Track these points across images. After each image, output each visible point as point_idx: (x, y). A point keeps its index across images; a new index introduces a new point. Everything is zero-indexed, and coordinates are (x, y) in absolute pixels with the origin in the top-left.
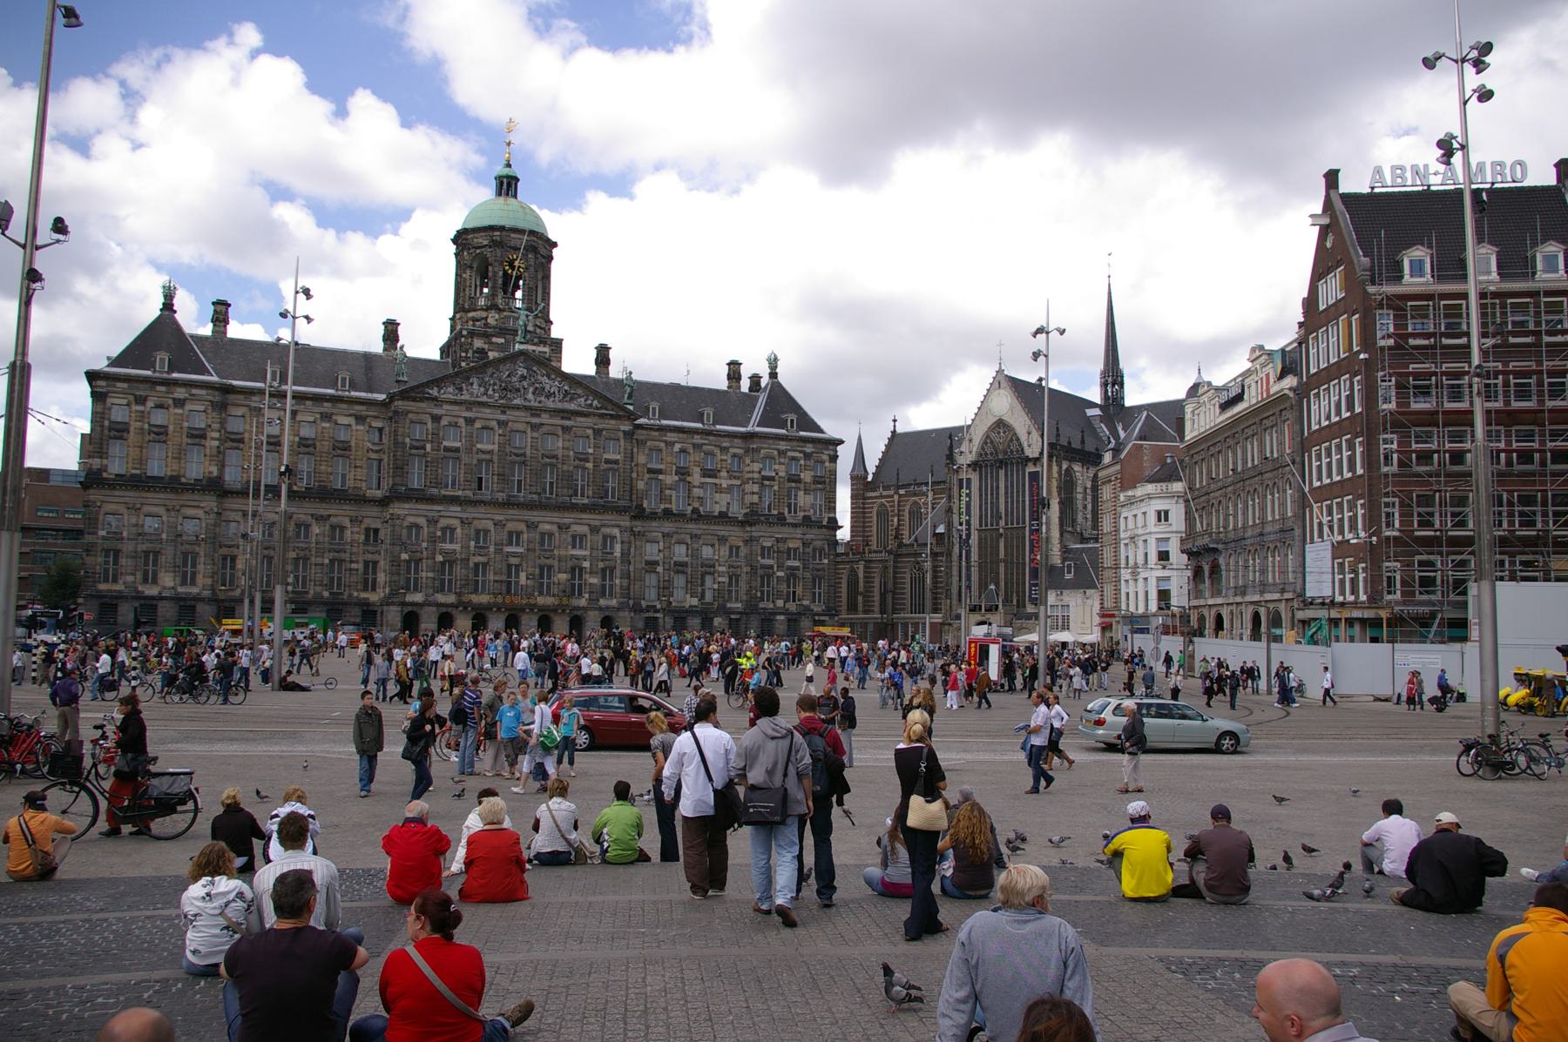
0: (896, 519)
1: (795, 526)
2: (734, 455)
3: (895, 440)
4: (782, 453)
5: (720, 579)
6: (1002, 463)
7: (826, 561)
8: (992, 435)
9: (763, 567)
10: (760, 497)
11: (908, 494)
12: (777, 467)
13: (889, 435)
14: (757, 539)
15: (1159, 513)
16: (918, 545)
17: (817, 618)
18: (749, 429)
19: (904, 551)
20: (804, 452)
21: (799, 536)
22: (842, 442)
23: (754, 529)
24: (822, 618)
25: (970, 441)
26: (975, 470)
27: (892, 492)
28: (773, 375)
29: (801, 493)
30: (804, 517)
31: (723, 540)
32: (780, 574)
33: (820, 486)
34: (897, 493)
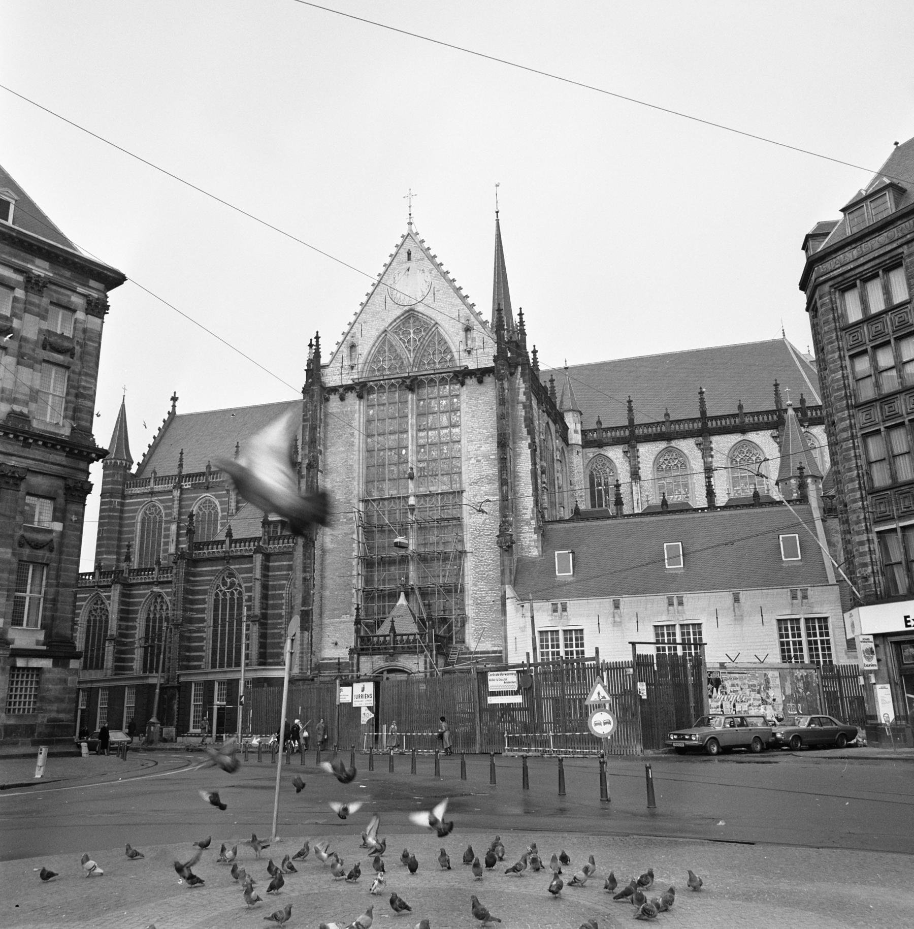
0: (174, 527)
3: (174, 425)
6: (413, 384)
8: (394, 339)
11: (195, 487)
13: (166, 417)
16: (232, 541)
17: (20, 663)
19: (206, 552)
22: (115, 279)
24: (35, 663)
25: (353, 347)
26: (360, 397)
27: (171, 486)
33: (59, 358)
34: (179, 486)
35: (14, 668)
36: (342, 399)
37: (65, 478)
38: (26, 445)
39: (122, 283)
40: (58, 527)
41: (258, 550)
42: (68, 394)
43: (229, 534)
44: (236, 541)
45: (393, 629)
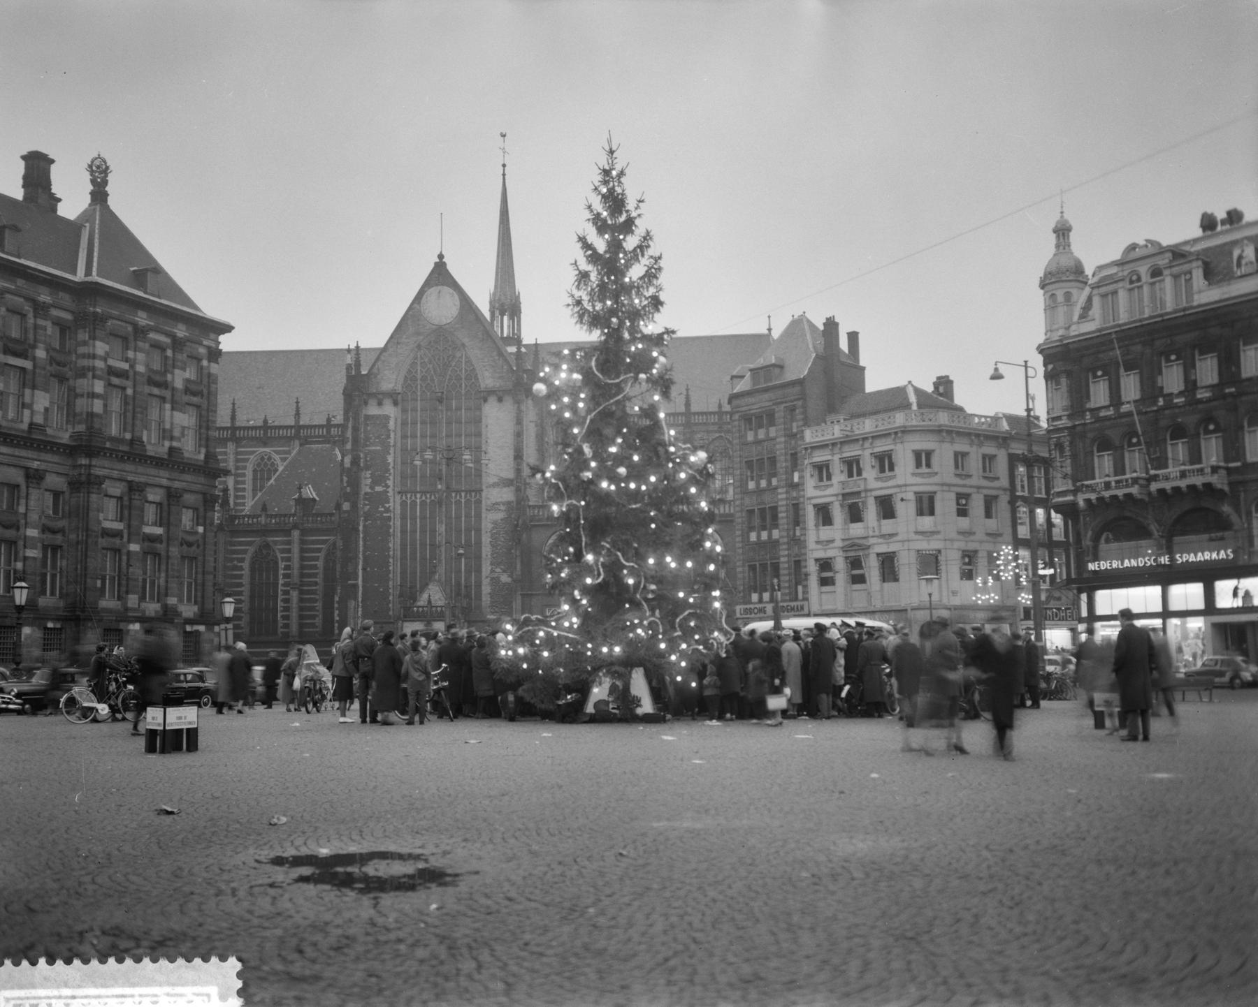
1: (158, 462)
2: (57, 322)
4: (140, 332)
5: (30, 553)
7: (201, 529)
9: (107, 533)
10: (105, 406)
12: (130, 354)
14: (99, 481)
15: (917, 454)
17: (188, 628)
18: (80, 276)
20: (173, 337)
21: (165, 482)
22: (227, 328)
23: (94, 462)
28: (99, 194)
29: (168, 406)
30: (171, 449)
31: (34, 477)
32: (134, 547)
33: (195, 400)
35: (185, 632)
36: (380, 404)
37: (204, 494)
38: (183, 472)
39: (230, 331)
40: (201, 529)
41: (295, 527)
42: (200, 428)
43: (264, 508)
44: (271, 516)
45: (429, 602)
